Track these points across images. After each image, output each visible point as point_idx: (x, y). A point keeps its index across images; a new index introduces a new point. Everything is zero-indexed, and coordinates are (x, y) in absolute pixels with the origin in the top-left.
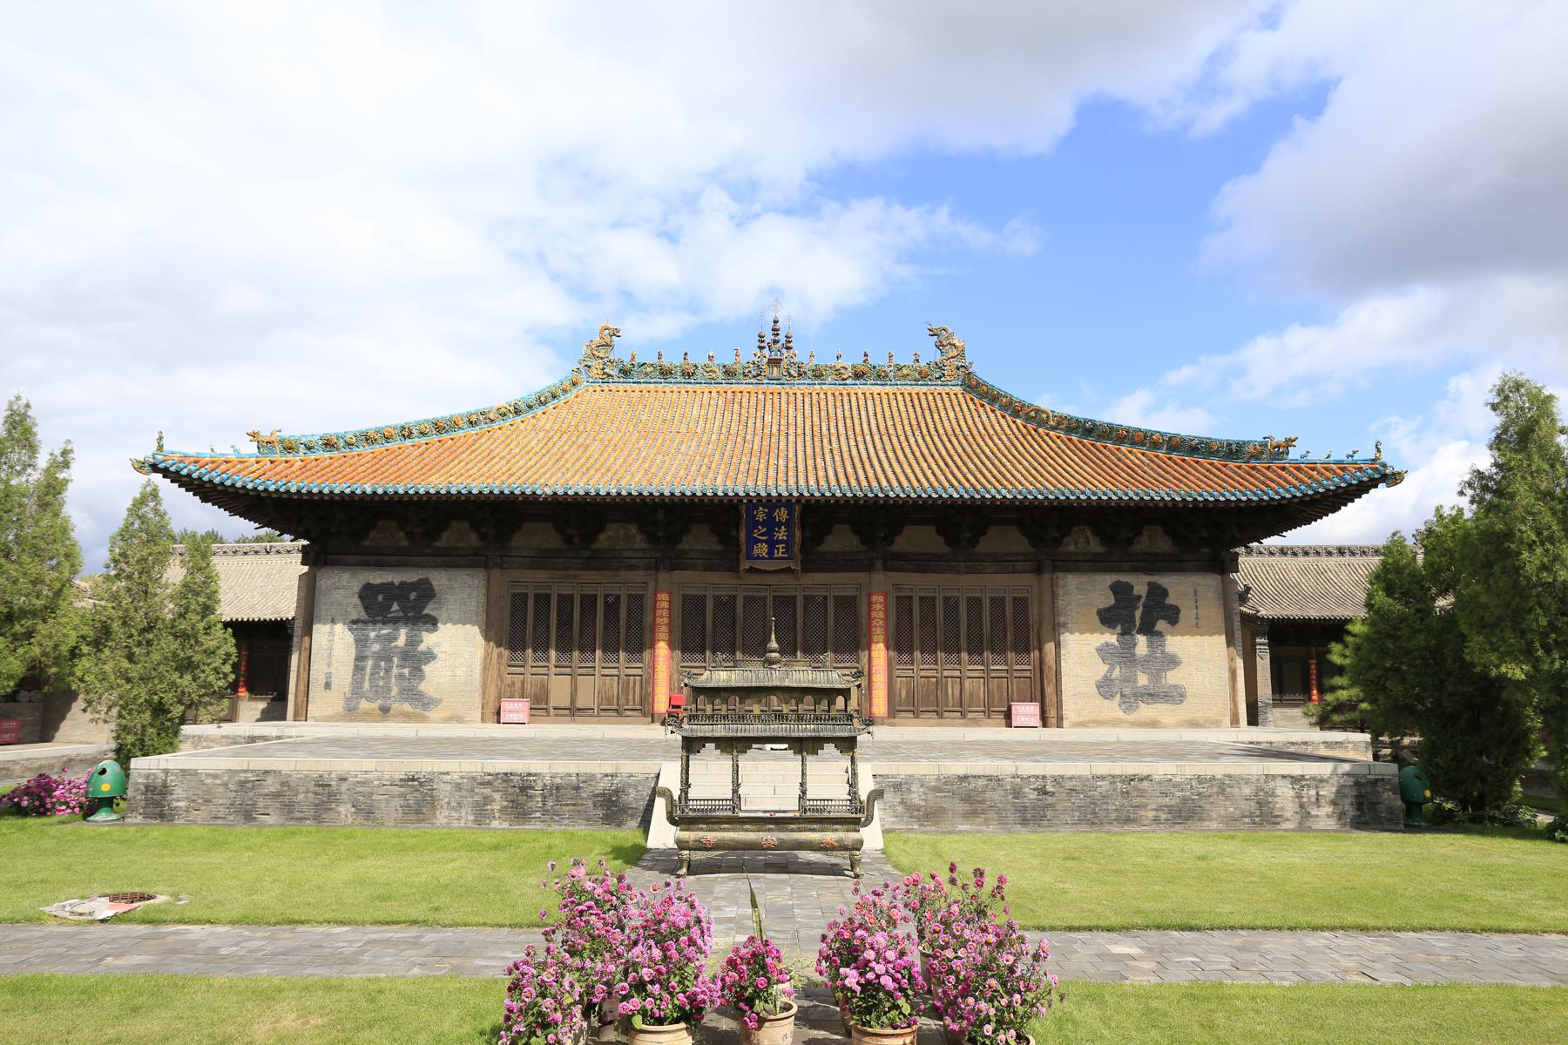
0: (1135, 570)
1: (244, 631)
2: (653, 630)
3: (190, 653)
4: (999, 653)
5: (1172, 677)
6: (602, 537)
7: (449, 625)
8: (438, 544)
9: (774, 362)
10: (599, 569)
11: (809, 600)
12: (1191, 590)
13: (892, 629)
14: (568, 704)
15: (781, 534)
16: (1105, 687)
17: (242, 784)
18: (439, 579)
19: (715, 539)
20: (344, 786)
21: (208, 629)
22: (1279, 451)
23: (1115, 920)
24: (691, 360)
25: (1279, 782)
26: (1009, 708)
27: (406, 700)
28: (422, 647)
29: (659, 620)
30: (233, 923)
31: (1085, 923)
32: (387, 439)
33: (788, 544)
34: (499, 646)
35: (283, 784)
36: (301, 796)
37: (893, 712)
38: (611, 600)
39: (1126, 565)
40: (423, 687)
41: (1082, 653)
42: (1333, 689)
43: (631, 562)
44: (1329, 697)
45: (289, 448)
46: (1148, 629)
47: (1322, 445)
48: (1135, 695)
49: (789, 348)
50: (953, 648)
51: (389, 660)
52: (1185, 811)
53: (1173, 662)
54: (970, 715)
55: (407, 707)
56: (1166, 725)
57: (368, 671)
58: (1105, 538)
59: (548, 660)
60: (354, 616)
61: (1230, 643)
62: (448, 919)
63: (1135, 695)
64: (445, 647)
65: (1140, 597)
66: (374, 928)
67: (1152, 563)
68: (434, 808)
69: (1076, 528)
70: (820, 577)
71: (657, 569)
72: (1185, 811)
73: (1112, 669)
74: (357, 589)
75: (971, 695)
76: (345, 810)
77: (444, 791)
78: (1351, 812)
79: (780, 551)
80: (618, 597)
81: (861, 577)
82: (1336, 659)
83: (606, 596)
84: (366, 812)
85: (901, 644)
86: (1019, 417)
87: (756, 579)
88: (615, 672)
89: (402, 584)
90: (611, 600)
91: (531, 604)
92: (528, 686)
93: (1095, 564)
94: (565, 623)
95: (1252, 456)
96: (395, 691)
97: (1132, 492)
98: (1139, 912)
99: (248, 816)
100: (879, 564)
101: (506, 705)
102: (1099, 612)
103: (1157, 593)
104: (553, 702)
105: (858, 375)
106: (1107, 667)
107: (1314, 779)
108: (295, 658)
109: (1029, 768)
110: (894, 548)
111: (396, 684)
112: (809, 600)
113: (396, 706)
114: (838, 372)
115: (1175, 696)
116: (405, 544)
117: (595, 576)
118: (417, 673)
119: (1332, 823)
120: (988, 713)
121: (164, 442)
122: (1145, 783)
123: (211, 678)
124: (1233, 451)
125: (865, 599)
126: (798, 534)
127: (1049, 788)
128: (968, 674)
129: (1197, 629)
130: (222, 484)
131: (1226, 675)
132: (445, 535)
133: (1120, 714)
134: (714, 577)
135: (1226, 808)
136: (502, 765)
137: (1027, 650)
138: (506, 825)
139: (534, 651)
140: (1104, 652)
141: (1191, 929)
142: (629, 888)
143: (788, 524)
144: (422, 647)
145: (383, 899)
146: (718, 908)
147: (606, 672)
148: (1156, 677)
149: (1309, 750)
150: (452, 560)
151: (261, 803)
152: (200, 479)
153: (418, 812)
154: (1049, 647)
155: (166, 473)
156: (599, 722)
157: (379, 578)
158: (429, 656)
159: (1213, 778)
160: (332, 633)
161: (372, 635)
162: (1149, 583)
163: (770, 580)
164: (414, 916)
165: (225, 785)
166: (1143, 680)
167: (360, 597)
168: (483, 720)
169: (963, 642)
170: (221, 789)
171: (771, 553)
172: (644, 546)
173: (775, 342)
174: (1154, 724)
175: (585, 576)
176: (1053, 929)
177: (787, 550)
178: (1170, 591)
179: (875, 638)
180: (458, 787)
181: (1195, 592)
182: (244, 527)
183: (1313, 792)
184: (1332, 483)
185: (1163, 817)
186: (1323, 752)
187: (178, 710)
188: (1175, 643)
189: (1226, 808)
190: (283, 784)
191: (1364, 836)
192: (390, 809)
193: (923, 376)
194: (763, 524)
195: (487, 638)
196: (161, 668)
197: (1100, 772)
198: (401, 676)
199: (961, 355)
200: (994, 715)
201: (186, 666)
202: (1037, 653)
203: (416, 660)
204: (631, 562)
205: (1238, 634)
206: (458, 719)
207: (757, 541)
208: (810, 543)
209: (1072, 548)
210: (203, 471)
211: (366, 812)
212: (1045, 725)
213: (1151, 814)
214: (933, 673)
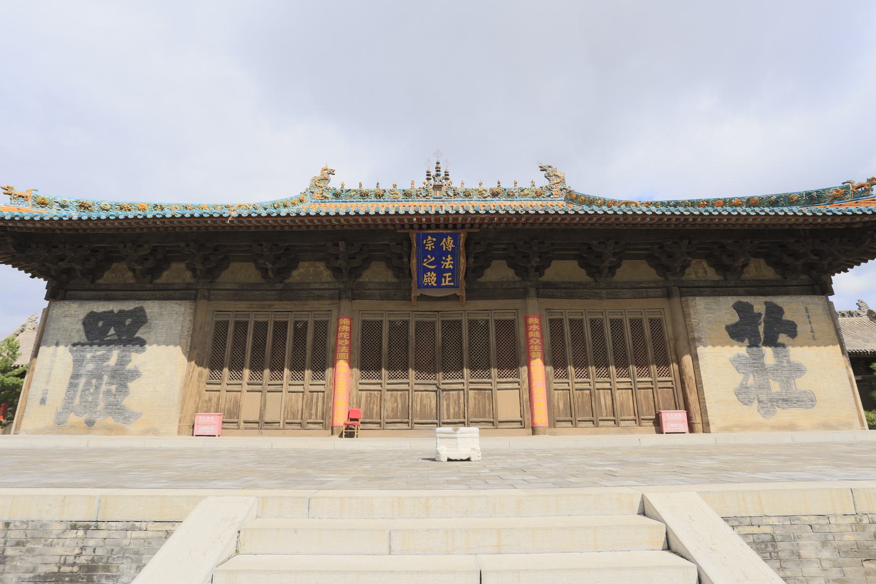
2: (335, 351)
4: (642, 367)
5: (802, 384)
6: (295, 273)
7: (155, 346)
8: (158, 281)
9: (438, 187)
10: (290, 299)
11: (472, 323)
12: (802, 308)
13: (547, 347)
14: (257, 419)
15: (448, 264)
18: (151, 308)
24: (382, 187)
27: (110, 414)
28: (130, 367)
29: (340, 342)
33: (454, 271)
34: (199, 364)
37: (554, 422)
38: (299, 326)
39: (740, 290)
41: (718, 363)
43: (317, 293)
46: (771, 341)
48: (771, 401)
49: (446, 179)
50: (602, 363)
51: (100, 378)
53: (798, 370)
54: (622, 423)
55: (110, 421)
57: (81, 387)
58: (720, 267)
59: (241, 378)
60: (76, 340)
63: (771, 401)
65: (760, 315)
67: (760, 288)
70: (481, 304)
71: (340, 299)
73: (746, 377)
75: (622, 405)
79: (447, 281)
80: (306, 323)
81: (517, 303)
83: (296, 322)
85: (557, 361)
87: (425, 306)
88: (300, 388)
89: (121, 312)
90: (299, 326)
91: (231, 328)
92: (222, 402)
93: (715, 290)
94: (259, 346)
96: (101, 405)
100: (532, 291)
101: (200, 419)
102: (728, 328)
103: (774, 312)
104: (244, 416)
105: (495, 194)
110: (545, 278)
111: (103, 402)
112: (472, 323)
113: (100, 420)
114: (481, 193)
115: (807, 401)
116: (132, 281)
117: (287, 305)
118: (123, 388)
120: (638, 420)
126: (462, 260)
128: (617, 387)
129: (814, 340)
132: (165, 274)
133: (759, 418)
134: (390, 305)
139: (230, 370)
140: (737, 362)
143: (454, 253)
144: (130, 367)
148: (787, 383)
150: (167, 293)
154: (687, 359)
156: (283, 435)
157: (100, 307)
158: (135, 374)
160: (54, 354)
161: (89, 356)
162: (766, 303)
166: (776, 387)
167: (84, 323)
168: (179, 432)
169: (611, 357)
171: (439, 281)
172: (330, 279)
173: (438, 175)
174: (792, 427)
175: (279, 305)
177: (454, 278)
178: (785, 309)
179: (533, 355)
181: (806, 310)
188: (797, 353)
193: (538, 195)
194: (432, 253)
195: (190, 359)
198: (108, 392)
199: (563, 181)
200: (644, 423)
202: (676, 366)
203: (122, 377)
204: (317, 293)
206: (152, 431)
207: (427, 270)
208: (474, 272)
209: (693, 277)
214: (586, 386)
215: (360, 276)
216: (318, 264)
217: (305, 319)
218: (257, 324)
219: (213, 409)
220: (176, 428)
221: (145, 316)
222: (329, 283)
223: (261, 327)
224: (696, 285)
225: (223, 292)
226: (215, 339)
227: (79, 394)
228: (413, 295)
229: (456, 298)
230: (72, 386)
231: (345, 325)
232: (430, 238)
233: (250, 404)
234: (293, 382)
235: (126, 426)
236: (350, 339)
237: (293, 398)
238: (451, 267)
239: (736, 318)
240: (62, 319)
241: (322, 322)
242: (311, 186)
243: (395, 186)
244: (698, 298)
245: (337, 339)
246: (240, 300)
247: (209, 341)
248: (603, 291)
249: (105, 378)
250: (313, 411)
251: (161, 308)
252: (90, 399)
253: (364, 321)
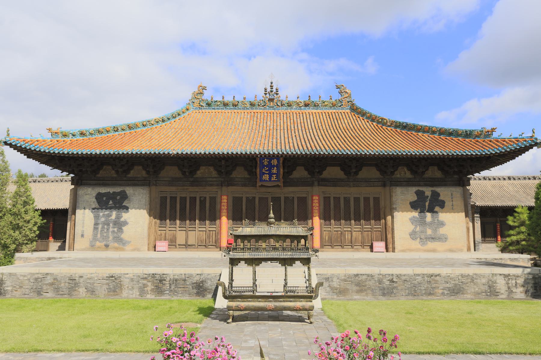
0: (426, 185)
1: (45, 213)
3: (18, 222)
4: (367, 221)
5: (442, 231)
6: (198, 172)
7: (133, 210)
8: (129, 176)
9: (271, 100)
11: (286, 198)
12: (450, 194)
14: (184, 243)
15: (275, 171)
16: (413, 235)
17: (36, 279)
18: (129, 190)
19: (246, 173)
20: (82, 280)
21: (26, 212)
22: (488, 134)
23: (441, 349)
24: (236, 99)
25: (498, 276)
26: (372, 244)
28: (122, 219)
29: (223, 207)
30: (6, 351)
31: (426, 350)
32: (108, 132)
33: (277, 174)
34: (155, 218)
35: (54, 279)
36: (63, 285)
37: (322, 246)
38: (202, 199)
39: (422, 183)
40: (123, 236)
41: (403, 221)
42: (509, 236)
43: (211, 183)
44: (508, 239)
45: (65, 136)
46: (431, 210)
47: (508, 131)
48: (426, 238)
49: (277, 94)
50: (348, 218)
51: (108, 225)
52: (456, 290)
53: (442, 224)
54: (355, 247)
55: (116, 245)
56: (440, 251)
57: (100, 230)
59: (176, 224)
60: (94, 206)
61: (467, 216)
62: (112, 348)
63: (426, 238)
65: (428, 197)
66: (76, 354)
67: (433, 182)
68: (121, 289)
69: (400, 168)
70: (291, 189)
71: (222, 186)
72: (456, 290)
74: (94, 195)
75: (356, 239)
76: (82, 290)
77: (126, 282)
78: (532, 290)
79: (274, 178)
80: (205, 198)
81: (309, 189)
82: (511, 223)
83: (200, 197)
84: (92, 291)
85: (326, 217)
86: (374, 122)
87: (263, 190)
88: (204, 229)
89: (114, 192)
90: (202, 199)
91: (168, 200)
92: (167, 235)
93: (408, 183)
95: (477, 136)
96: (111, 238)
97: (426, 151)
98: (450, 343)
99: (39, 293)
100: (316, 183)
101: (158, 244)
102: (411, 203)
103: (436, 195)
104: (178, 242)
105: (306, 105)
106: (414, 227)
107: (514, 276)
108: (69, 224)
109: (386, 271)
112: (286, 198)
113: (112, 244)
114: (298, 104)
115: (443, 239)
116: (115, 176)
117: (196, 189)
118: (120, 230)
119: (523, 296)
120: (363, 246)
121: (10, 132)
122: (438, 277)
123: (28, 233)
124: (468, 134)
125: (310, 198)
126: (282, 170)
127: (395, 280)
128: (354, 230)
129: (453, 210)
130: (35, 150)
131: (465, 230)
132: (132, 172)
133: (419, 246)
135: (474, 288)
136: (152, 270)
137: (380, 220)
138: (153, 297)
139: (170, 221)
140: (413, 220)
141: (480, 353)
142: (197, 339)
143: (277, 166)
144: (122, 219)
145: (85, 337)
146: (246, 341)
147: (200, 229)
148: (435, 230)
149: (503, 262)
150: (135, 183)
151: (45, 287)
152: (25, 148)
153: (114, 291)
154: (389, 218)
155: (11, 145)
156: (197, 251)
157: (104, 190)
158: (125, 223)
159: (469, 275)
160: (84, 214)
161: (101, 214)
162: (432, 191)
163: (270, 190)
164: (98, 346)
165: (29, 280)
166: (429, 232)
167: (96, 198)
169: (352, 216)
170: (27, 282)
171: (270, 178)
172: (216, 176)
173: (272, 91)
174: (434, 251)
175: (191, 189)
176: (410, 353)
177: (277, 177)
178: (441, 194)
179: (315, 215)
180: (132, 280)
181: (452, 194)
182: (46, 169)
183: (514, 282)
184: (513, 147)
185: (446, 292)
186: (509, 262)
187: (13, 247)
188: (443, 216)
189: (474, 288)
190: (54, 279)
191: (536, 301)
192: (102, 290)
193: (334, 105)
194: (267, 166)
195: (150, 215)
196: (5, 229)
197: (417, 273)
198: (113, 231)
199: (350, 96)
200: (365, 247)
201: (16, 227)
202: (384, 221)
203: (119, 225)
204: (211, 183)
205: (470, 212)
206: (138, 250)
207: (264, 174)
209: (398, 176)
210: (27, 145)
211: (92, 291)
212: (387, 251)
213: (441, 291)
214: (339, 229)
215: (231, 174)
216: (210, 168)
217: (205, 196)
218: (181, 198)
219: (163, 239)
220: (147, 248)
221: (126, 195)
222: (216, 178)
223: (183, 200)
226: (161, 205)
227: (99, 232)
228: (258, 185)
229: (278, 186)
230: (95, 229)
231: (225, 199)
233: (181, 237)
234: (200, 226)
235: (124, 247)
236: (227, 206)
239: (415, 198)
240: (85, 196)
242: (192, 98)
243: (244, 98)
244: (398, 188)
245: (221, 206)
247: (158, 206)
248: (352, 183)
249: (111, 225)
250: (211, 240)
251: (134, 191)
252: (105, 235)
253: (233, 197)
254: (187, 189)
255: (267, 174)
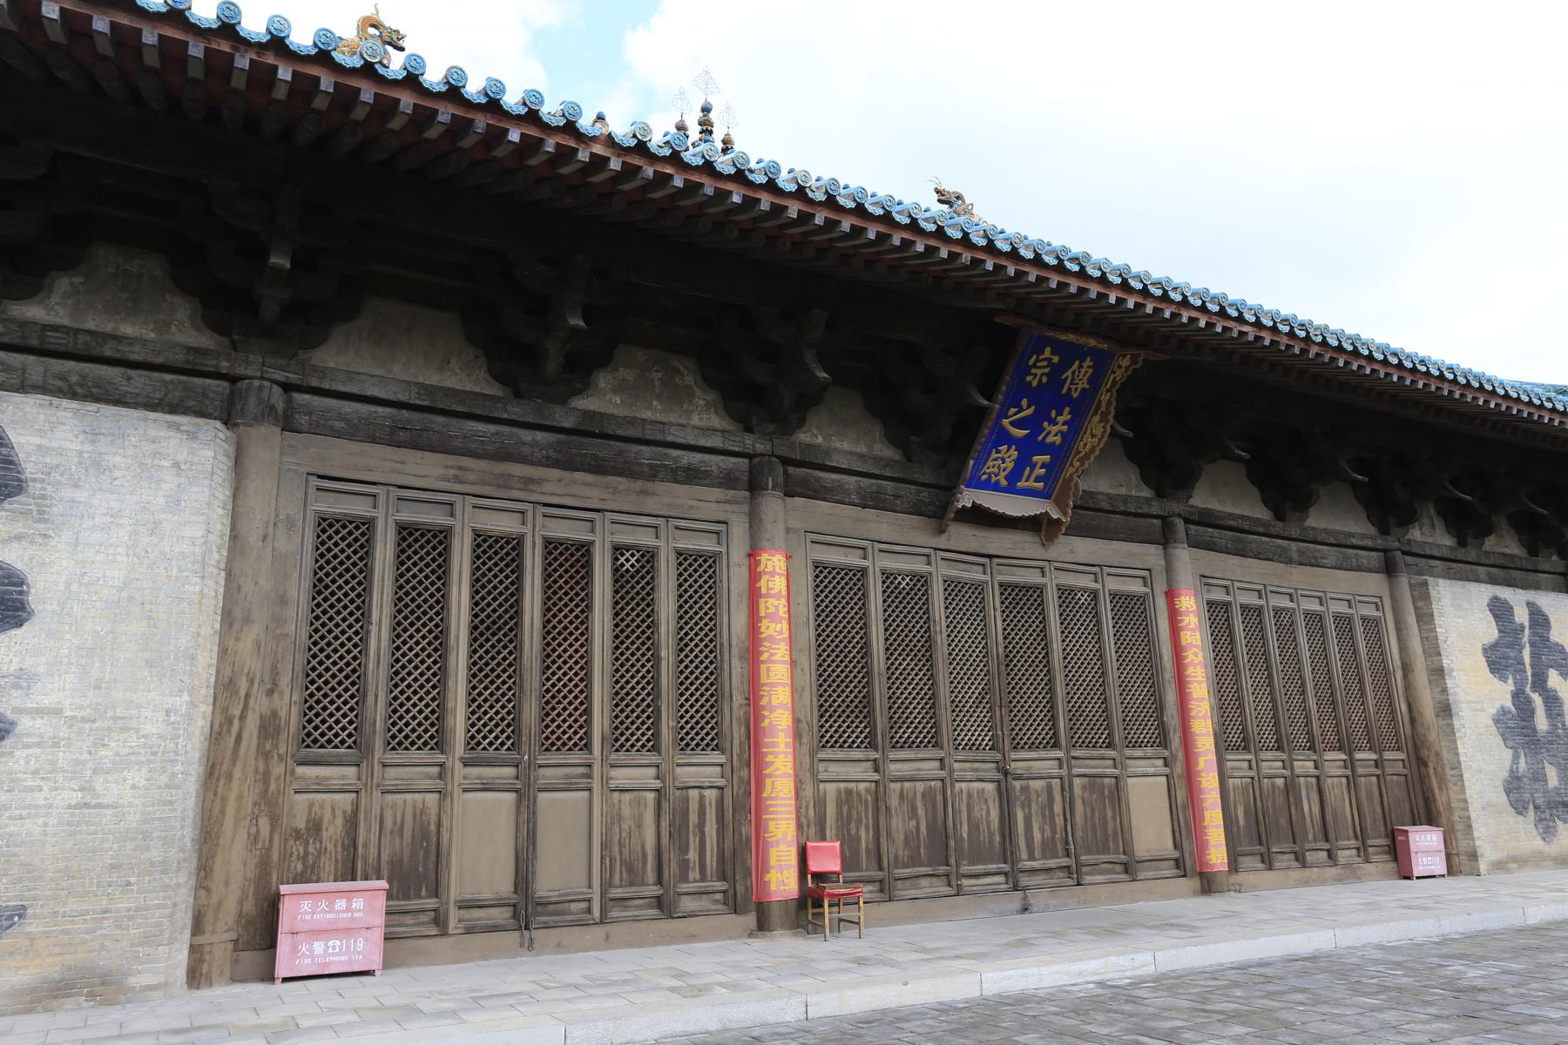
6: (603, 380)
10: (598, 468)
11: (1065, 593)
38: (629, 562)
64: (58, 690)
71: (754, 487)
80: (649, 557)
83: (618, 549)
90: (629, 562)
92: (367, 833)
94: (496, 624)
101: (302, 909)
102: (1485, 650)
104: (458, 884)
134: (884, 525)
147: (621, 776)
150: (89, 371)
156: (607, 943)
163: (996, 541)
168: (196, 976)
171: (1014, 476)
175: (558, 484)
194: (1035, 395)
207: (1004, 438)
217: (645, 539)
218: (485, 544)
219: (328, 865)
220: (182, 957)
221: (9, 463)
223: (499, 555)
224: (1428, 552)
225: (348, 407)
232: (1048, 351)
234: (621, 756)
237: (626, 811)
238: (1058, 439)
241: (699, 555)
246: (416, 446)
247: (299, 591)
250: (693, 855)
253: (816, 565)
254: (529, 481)
255: (1019, 443)
